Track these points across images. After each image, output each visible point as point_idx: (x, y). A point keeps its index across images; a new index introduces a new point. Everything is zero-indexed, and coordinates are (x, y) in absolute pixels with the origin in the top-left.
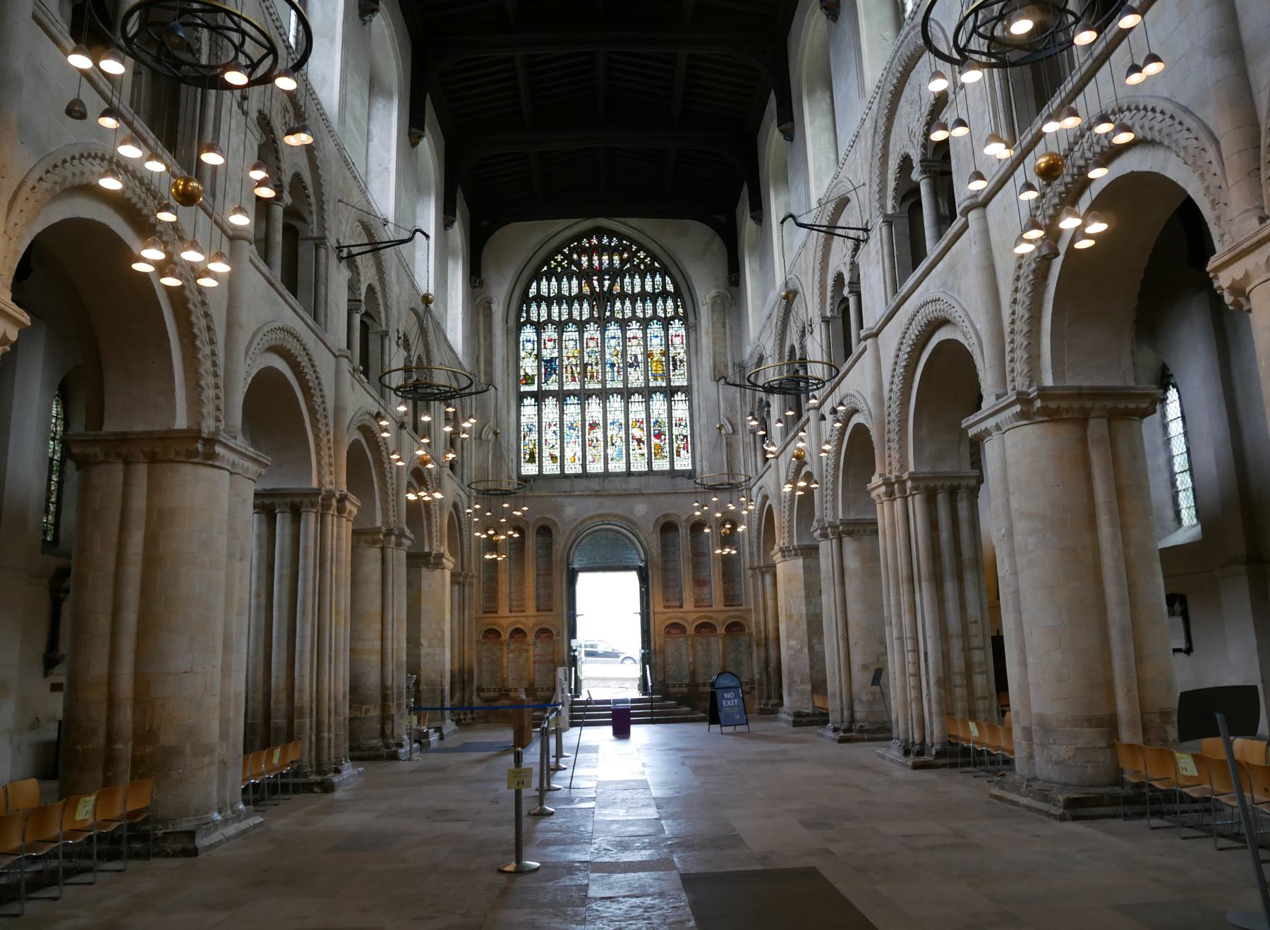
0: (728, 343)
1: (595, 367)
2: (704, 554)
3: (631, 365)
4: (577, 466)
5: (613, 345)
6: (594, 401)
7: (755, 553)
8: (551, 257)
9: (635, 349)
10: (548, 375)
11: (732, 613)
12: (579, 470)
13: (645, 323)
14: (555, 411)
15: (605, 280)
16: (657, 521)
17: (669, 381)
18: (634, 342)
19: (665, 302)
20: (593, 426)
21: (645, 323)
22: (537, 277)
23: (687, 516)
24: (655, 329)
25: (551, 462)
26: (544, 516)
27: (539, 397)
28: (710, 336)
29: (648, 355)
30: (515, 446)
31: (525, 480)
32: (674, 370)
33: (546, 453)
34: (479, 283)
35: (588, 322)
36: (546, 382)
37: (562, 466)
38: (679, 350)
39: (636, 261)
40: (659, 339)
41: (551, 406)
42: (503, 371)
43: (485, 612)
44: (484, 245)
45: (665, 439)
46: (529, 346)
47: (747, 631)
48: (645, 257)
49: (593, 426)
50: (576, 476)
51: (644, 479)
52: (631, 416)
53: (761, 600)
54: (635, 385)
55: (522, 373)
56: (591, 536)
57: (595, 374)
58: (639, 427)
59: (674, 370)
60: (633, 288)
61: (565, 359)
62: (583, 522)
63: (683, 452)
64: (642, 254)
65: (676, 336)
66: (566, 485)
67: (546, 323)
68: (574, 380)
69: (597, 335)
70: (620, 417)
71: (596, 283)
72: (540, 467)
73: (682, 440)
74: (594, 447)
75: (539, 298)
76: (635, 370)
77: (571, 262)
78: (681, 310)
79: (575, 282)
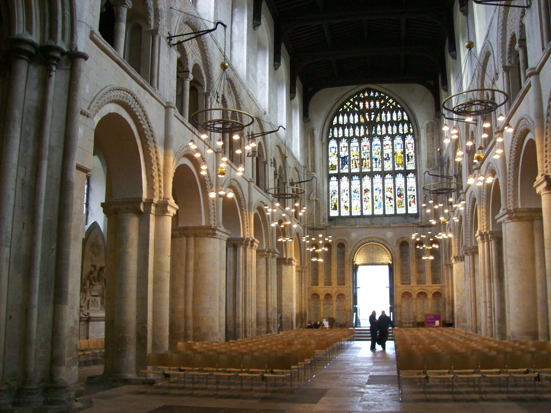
1: (367, 161)
3: (386, 159)
5: (376, 150)
8: (344, 103)
9: (388, 151)
10: (343, 165)
17: (405, 167)
18: (387, 147)
20: (366, 191)
22: (337, 114)
24: (398, 140)
27: (339, 176)
29: (394, 154)
30: (327, 202)
31: (331, 219)
33: (342, 204)
35: (363, 137)
36: (342, 168)
38: (410, 151)
39: (388, 104)
42: (320, 165)
43: (312, 285)
46: (333, 150)
47: (443, 297)
48: (393, 102)
49: (366, 191)
50: (358, 217)
51: (392, 218)
54: (387, 170)
55: (330, 164)
58: (390, 191)
60: (386, 118)
61: (352, 156)
64: (391, 101)
66: (353, 221)
67: (342, 138)
68: (356, 167)
69: (368, 144)
71: (367, 117)
74: (367, 202)
75: (338, 125)
77: (354, 106)
78: (411, 130)
79: (356, 116)
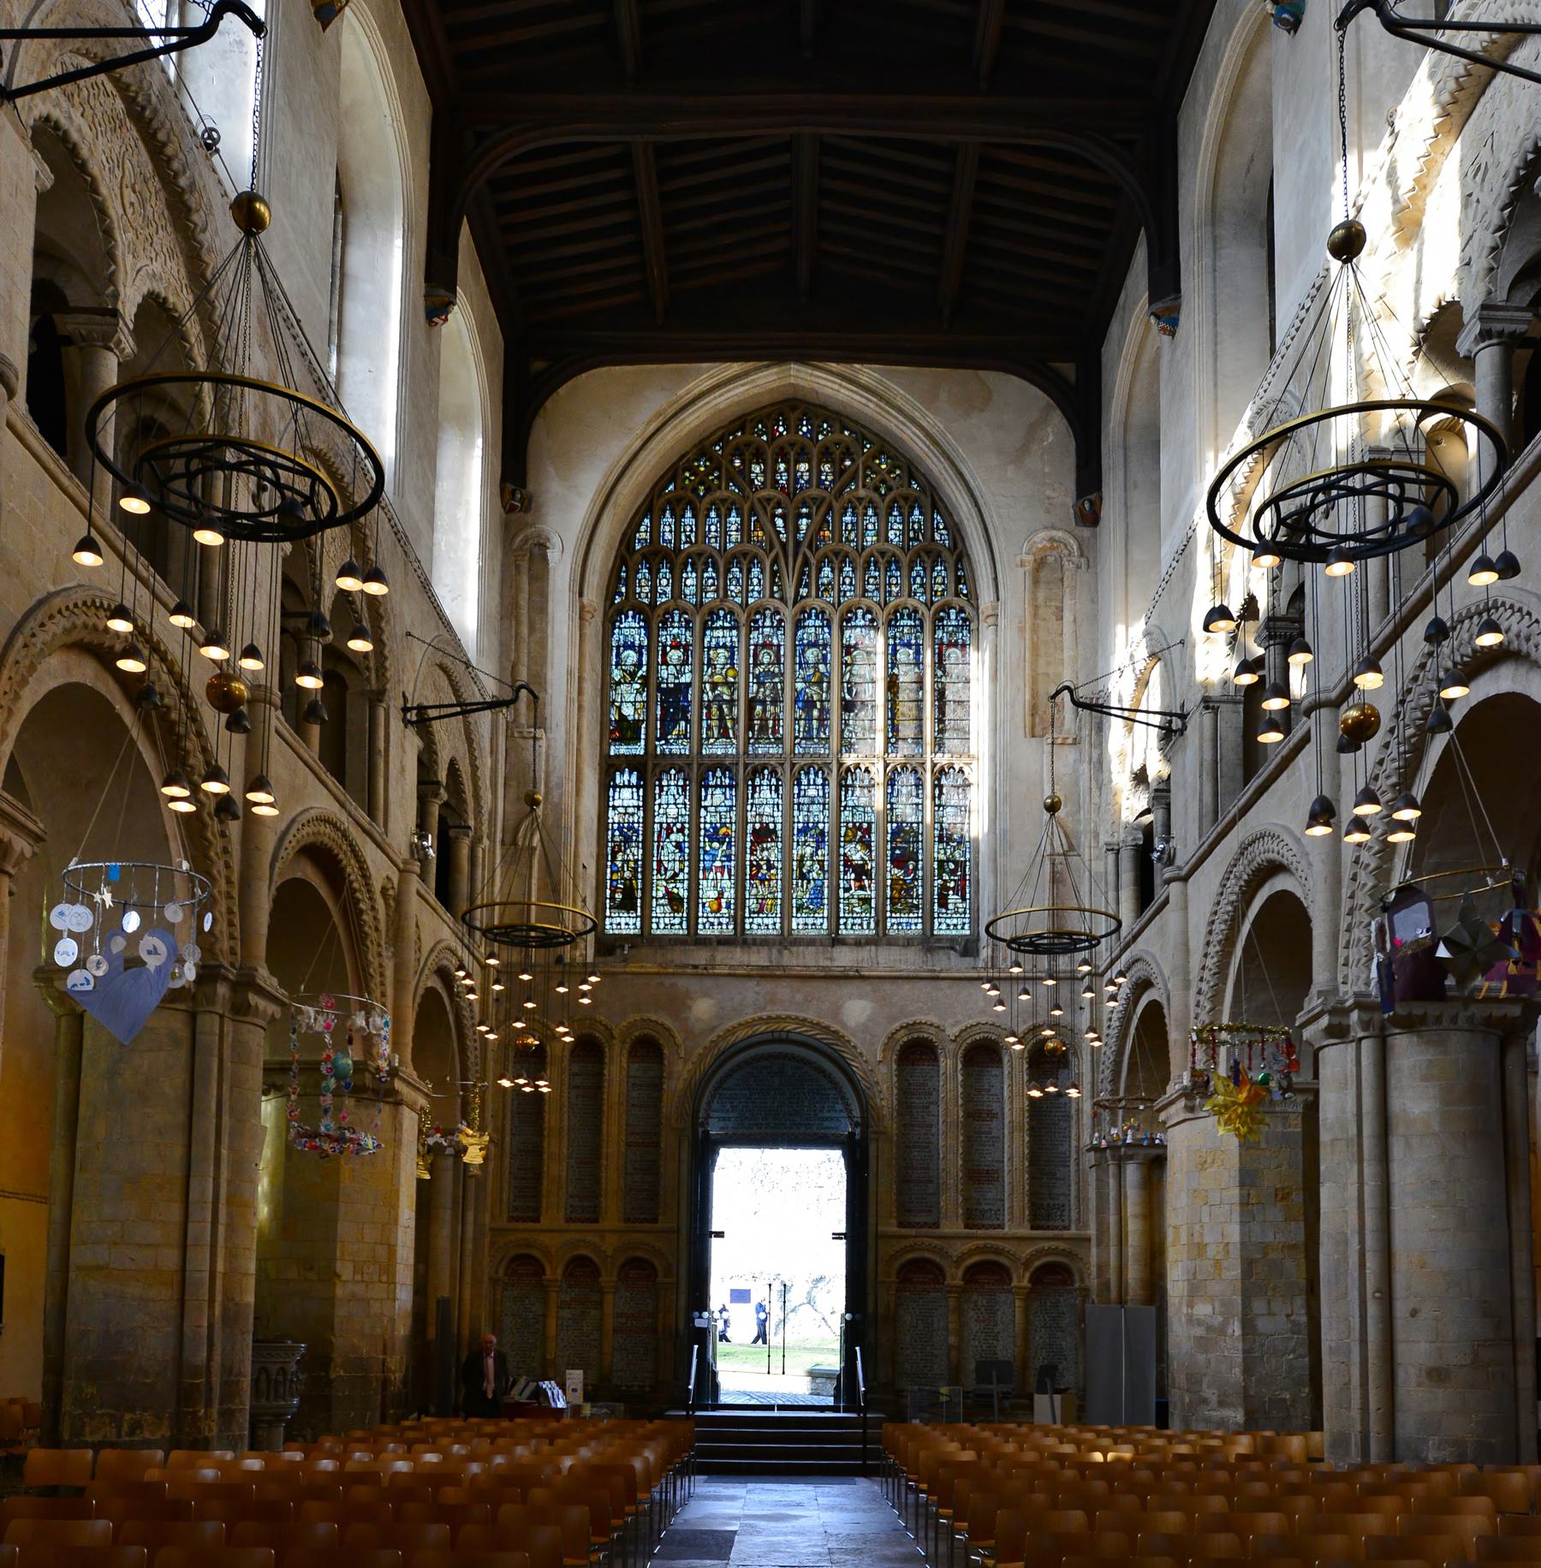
1: (771, 708)
2: (992, 1115)
4: (724, 921)
6: (765, 782)
10: (668, 722)
11: (1046, 1245)
12: (729, 930)
25: (668, 909)
26: (647, 1016)
27: (648, 772)
30: (592, 870)
34: (522, 500)
36: (664, 736)
37: (692, 920)
41: (673, 790)
43: (512, 1219)
44: (535, 414)
46: (630, 657)
47: (1077, 1285)
50: (722, 941)
53: (1112, 1219)
58: (861, 841)
66: (700, 957)
72: (646, 919)
73: (953, 872)
74: (762, 881)
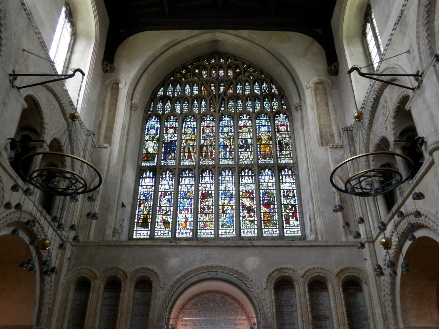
0: (332, 117)
3: (242, 147)
6: (207, 175)
7: (390, 315)
10: (167, 153)
12: (190, 235)
13: (255, 116)
14: (171, 182)
15: (221, 86)
16: (270, 276)
18: (245, 129)
19: (271, 101)
20: (206, 195)
21: (255, 116)
22: (164, 84)
23: (303, 271)
25: (163, 227)
28: (315, 111)
32: (280, 151)
33: (159, 219)
35: (205, 114)
36: (165, 159)
37: (174, 231)
40: (266, 128)
41: (168, 179)
45: (274, 208)
46: (153, 131)
49: (206, 195)
52: (242, 187)
56: (198, 298)
57: (209, 154)
58: (249, 197)
59: (280, 151)
62: (188, 274)
63: (292, 221)
65: (281, 125)
70: (231, 187)
72: (152, 231)
73: (291, 209)
74: (206, 214)
76: (245, 151)
